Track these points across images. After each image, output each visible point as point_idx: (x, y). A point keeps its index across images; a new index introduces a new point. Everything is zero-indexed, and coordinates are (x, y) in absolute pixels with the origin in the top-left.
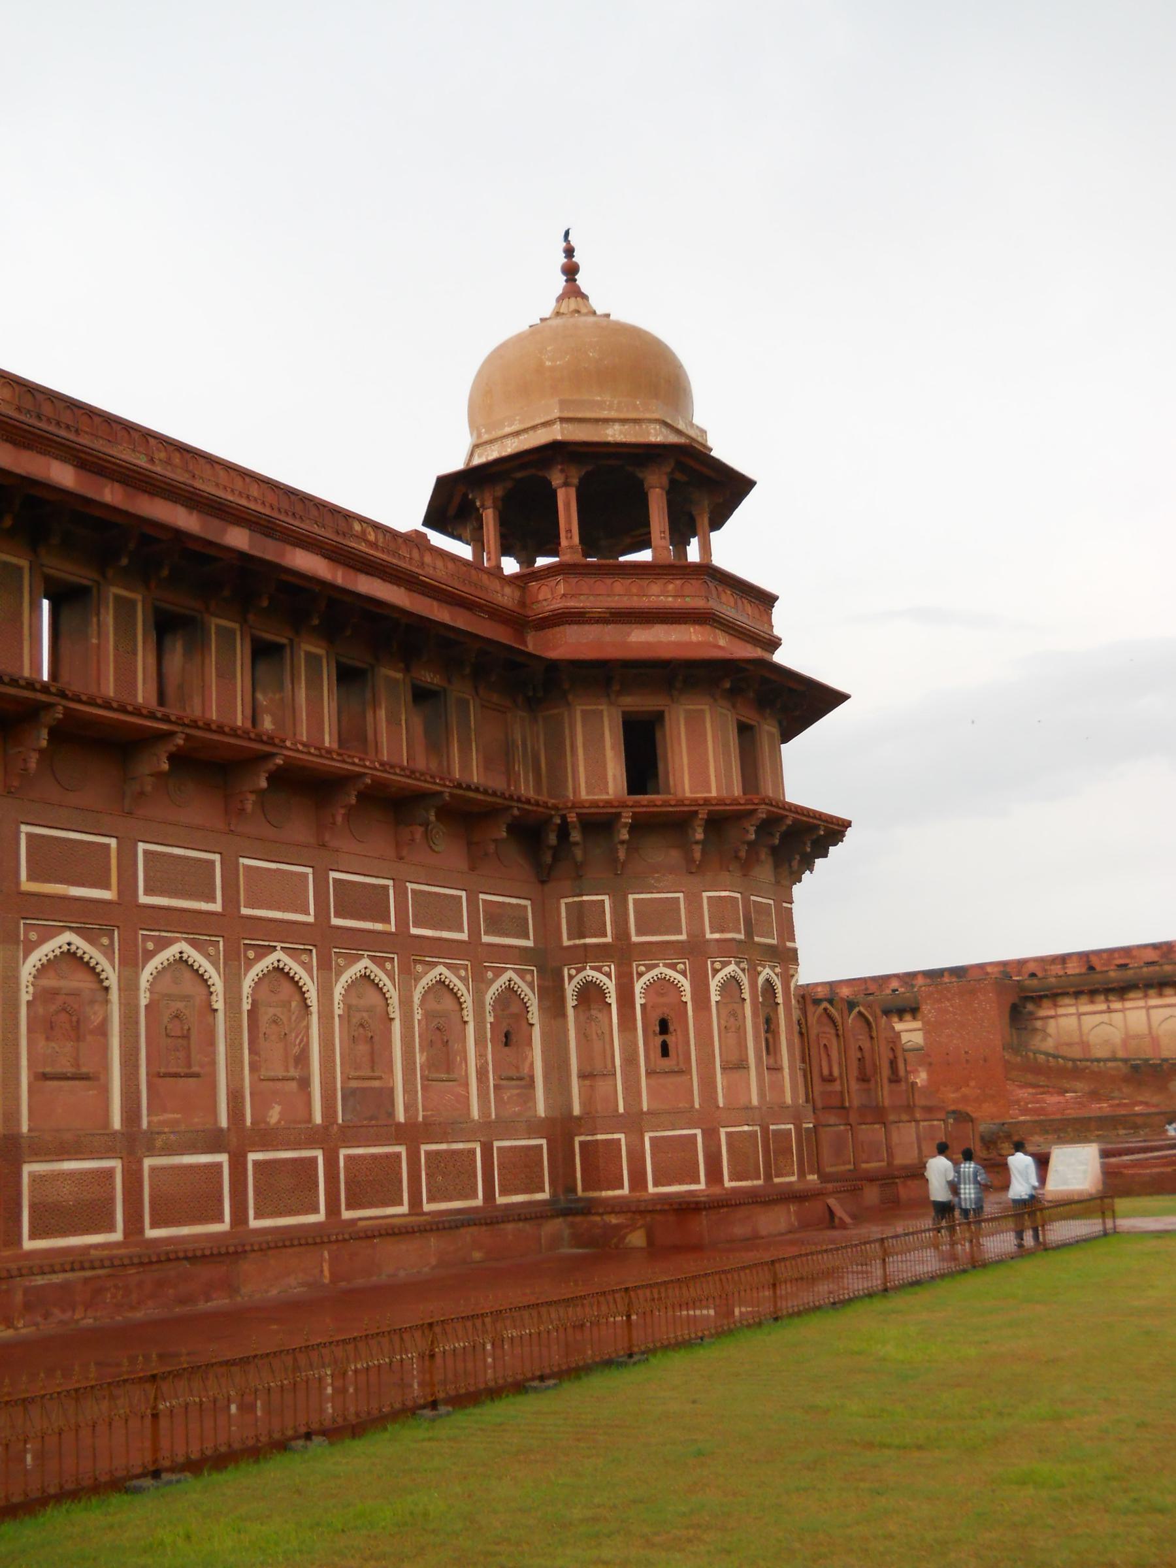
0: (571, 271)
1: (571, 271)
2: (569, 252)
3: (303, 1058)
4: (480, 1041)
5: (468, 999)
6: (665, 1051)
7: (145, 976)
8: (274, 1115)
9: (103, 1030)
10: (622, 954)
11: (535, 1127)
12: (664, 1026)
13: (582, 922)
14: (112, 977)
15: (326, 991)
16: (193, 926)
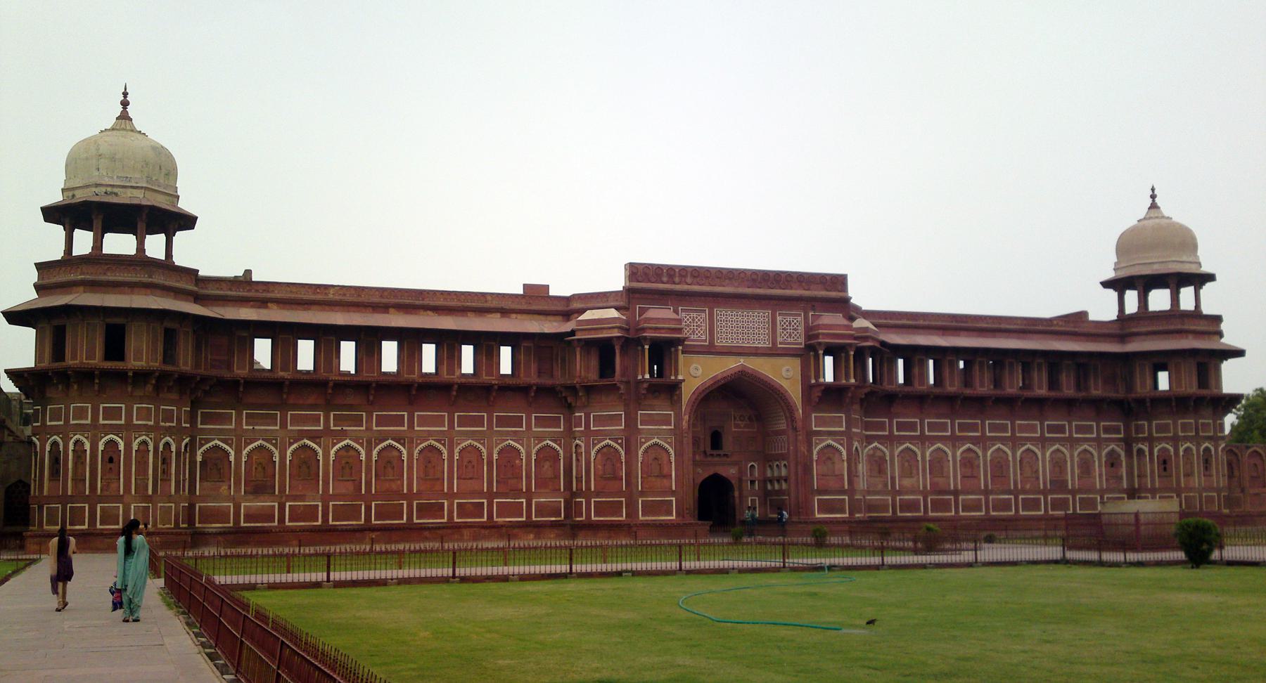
0: (1153, 197)
1: (1153, 197)
2: (1153, 190)
3: (1037, 471)
4: (1100, 466)
5: (1095, 454)
6: (1165, 469)
7: (989, 453)
8: (1028, 486)
9: (978, 466)
10: (1151, 440)
11: (1124, 491)
12: (1165, 462)
13: (1139, 429)
14: (980, 453)
15: (1044, 455)
16: (1003, 440)
